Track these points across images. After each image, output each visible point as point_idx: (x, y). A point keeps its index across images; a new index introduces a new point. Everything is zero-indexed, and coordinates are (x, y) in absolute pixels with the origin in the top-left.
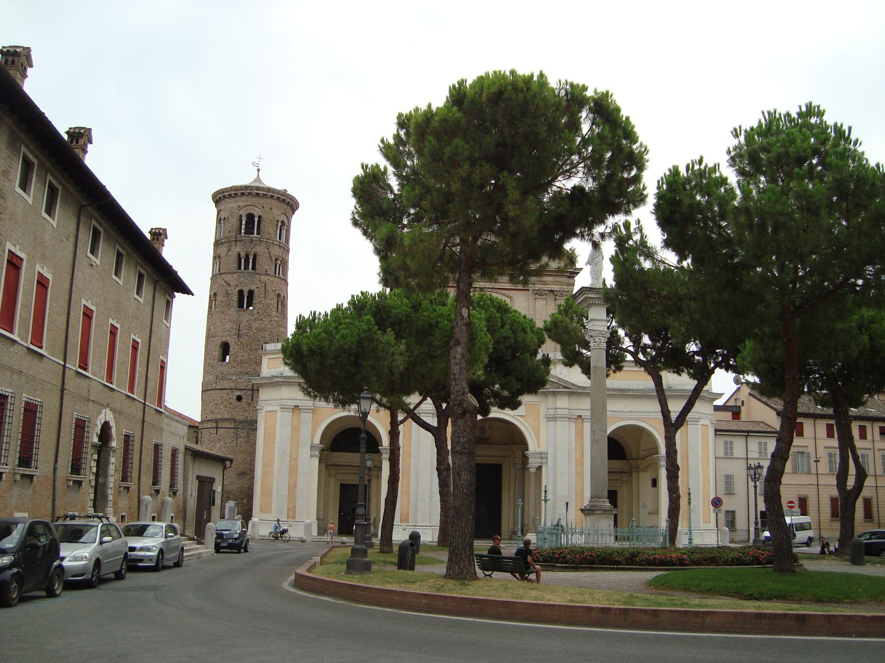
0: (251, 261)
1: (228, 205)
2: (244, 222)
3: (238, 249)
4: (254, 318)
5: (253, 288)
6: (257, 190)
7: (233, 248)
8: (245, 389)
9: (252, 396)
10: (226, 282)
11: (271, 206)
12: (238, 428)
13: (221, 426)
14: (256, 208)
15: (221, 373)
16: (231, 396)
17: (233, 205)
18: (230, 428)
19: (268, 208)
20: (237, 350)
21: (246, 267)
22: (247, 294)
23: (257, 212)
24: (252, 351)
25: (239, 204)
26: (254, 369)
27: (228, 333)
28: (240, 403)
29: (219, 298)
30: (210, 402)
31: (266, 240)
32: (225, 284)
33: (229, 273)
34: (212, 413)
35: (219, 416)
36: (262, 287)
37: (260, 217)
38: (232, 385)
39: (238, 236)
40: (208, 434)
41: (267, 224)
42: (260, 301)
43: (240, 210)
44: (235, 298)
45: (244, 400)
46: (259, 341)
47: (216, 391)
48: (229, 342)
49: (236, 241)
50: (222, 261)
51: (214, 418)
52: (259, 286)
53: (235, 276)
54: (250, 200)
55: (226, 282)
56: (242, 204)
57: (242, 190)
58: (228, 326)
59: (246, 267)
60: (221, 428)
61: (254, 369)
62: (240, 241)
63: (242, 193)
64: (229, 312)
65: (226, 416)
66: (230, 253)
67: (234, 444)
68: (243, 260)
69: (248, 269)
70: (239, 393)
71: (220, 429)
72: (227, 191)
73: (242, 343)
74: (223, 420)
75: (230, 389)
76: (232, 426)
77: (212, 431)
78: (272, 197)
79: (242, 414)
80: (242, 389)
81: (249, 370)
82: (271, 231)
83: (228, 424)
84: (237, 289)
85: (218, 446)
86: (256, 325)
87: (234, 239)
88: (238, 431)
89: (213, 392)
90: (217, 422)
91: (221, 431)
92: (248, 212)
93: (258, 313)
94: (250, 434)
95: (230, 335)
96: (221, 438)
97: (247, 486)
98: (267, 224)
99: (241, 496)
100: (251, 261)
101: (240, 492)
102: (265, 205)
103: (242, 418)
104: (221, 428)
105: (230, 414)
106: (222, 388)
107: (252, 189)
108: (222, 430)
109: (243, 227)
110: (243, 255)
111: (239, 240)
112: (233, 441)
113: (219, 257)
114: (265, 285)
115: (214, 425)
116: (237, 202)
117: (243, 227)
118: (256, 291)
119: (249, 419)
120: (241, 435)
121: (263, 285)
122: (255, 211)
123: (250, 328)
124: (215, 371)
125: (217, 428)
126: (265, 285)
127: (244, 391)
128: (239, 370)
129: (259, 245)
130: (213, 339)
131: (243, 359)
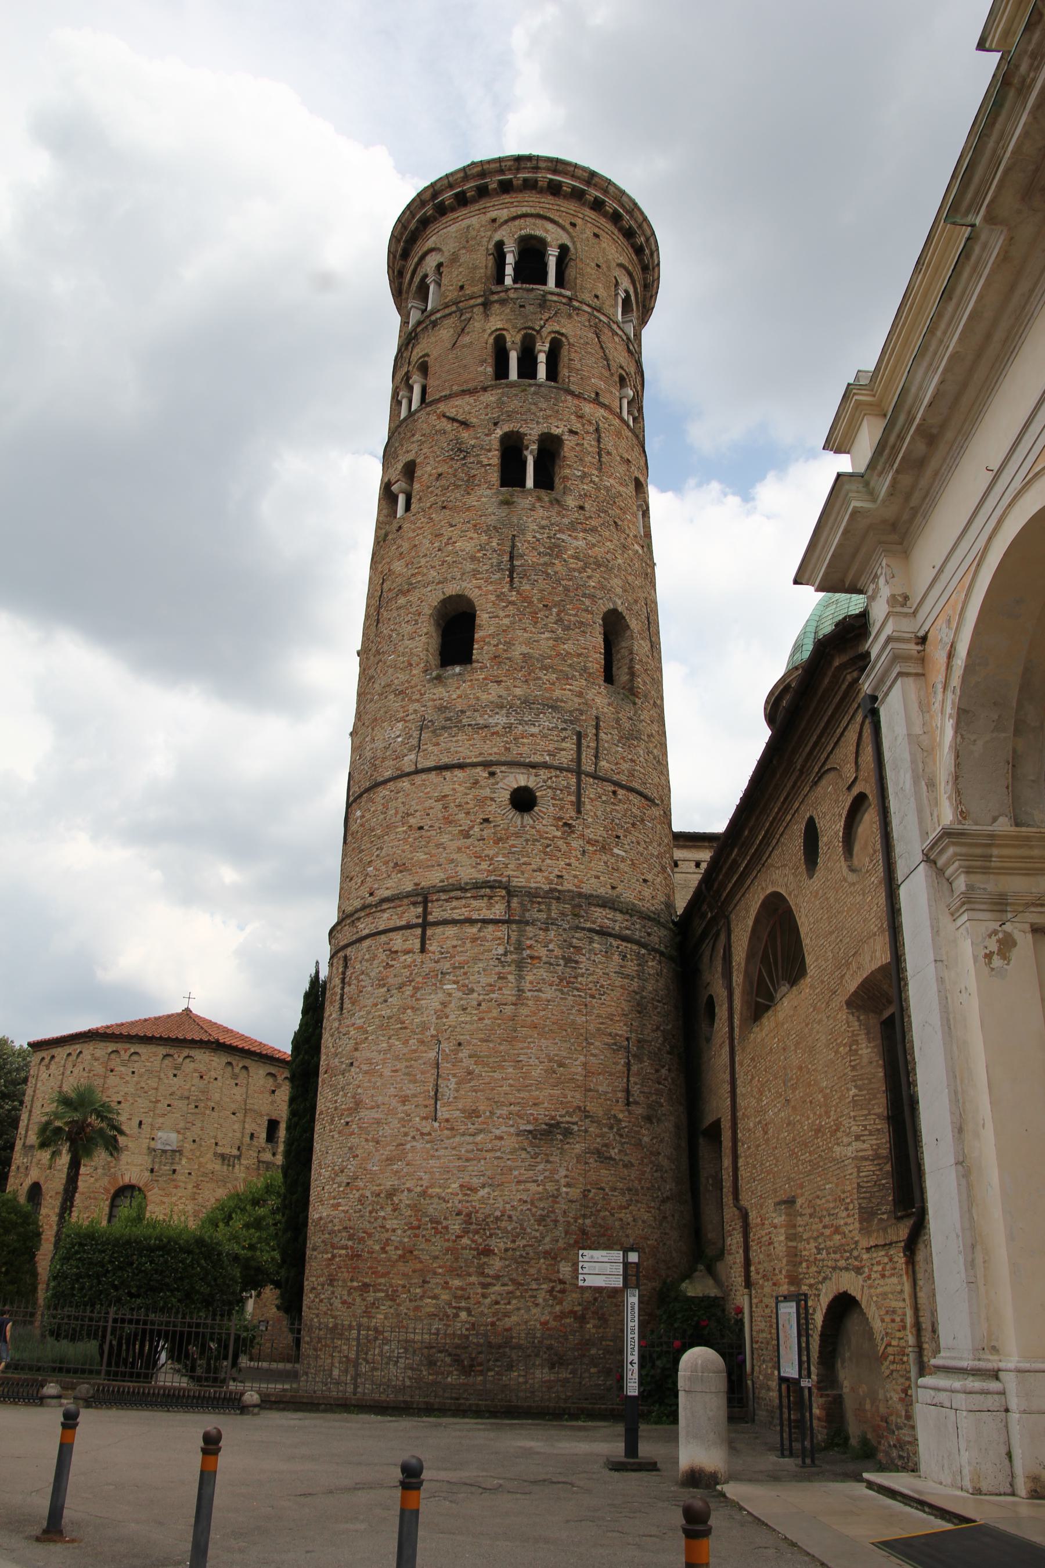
0: (542, 358)
1: (453, 228)
2: (510, 259)
3: (496, 323)
4: (566, 521)
5: (556, 431)
6: (555, 172)
7: (477, 324)
8: (545, 766)
9: (579, 796)
10: (453, 420)
11: (597, 231)
12: (523, 922)
13: (446, 915)
14: (550, 226)
15: (441, 709)
16: (487, 792)
17: (474, 221)
18: (485, 922)
19: (589, 233)
20: (506, 621)
21: (528, 369)
22: (534, 447)
23: (553, 236)
24: (567, 628)
25: (493, 214)
26: (580, 695)
27: (469, 566)
28: (527, 819)
29: (425, 472)
30: (389, 827)
31: (589, 310)
32: (448, 426)
33: (464, 392)
34: (400, 867)
35: (434, 877)
36: (587, 433)
37: (564, 249)
38: (492, 749)
39: (494, 288)
40: (382, 956)
41: (589, 270)
42: (585, 475)
43: (495, 230)
44: (494, 458)
45: (546, 807)
46: (592, 597)
47: (418, 779)
48: (474, 594)
49: (486, 305)
50: (432, 382)
51: (410, 887)
52: (577, 426)
53: (490, 397)
54: (529, 203)
55: (453, 420)
56: (504, 214)
57: (501, 171)
58: (466, 545)
59: (528, 369)
60: (445, 922)
61: (580, 695)
62: (503, 302)
63: (501, 183)
64: (472, 500)
65: (467, 873)
66: (466, 339)
67: (508, 993)
68: (513, 356)
69: (533, 375)
70: (521, 779)
71: (439, 930)
72: (451, 186)
73: (527, 599)
74: (456, 889)
75: (486, 764)
76: (498, 910)
77: (398, 941)
78: (597, 205)
79: (536, 862)
80: (533, 766)
81: (558, 693)
82: (601, 292)
83: (475, 903)
84: (499, 432)
85: (432, 1001)
86: (577, 543)
87: (480, 300)
88: (521, 933)
89: (405, 784)
90: (425, 902)
91: (443, 937)
92: (523, 232)
93: (582, 508)
94: (578, 949)
95: (475, 573)
96: (446, 966)
97: (575, 1193)
98: (589, 270)
99: (547, 1245)
100: (542, 358)
101: (541, 1220)
102: (579, 222)
103: (539, 882)
104: (445, 922)
105: (484, 866)
106: (445, 760)
107: (536, 169)
108: (451, 931)
109: (509, 270)
110: (513, 340)
111: (496, 301)
112: (501, 977)
113: (424, 368)
114: (597, 430)
115: (413, 914)
116: (484, 211)
117: (509, 270)
118: (569, 441)
119: (567, 886)
120: (542, 952)
121: (591, 429)
122: (547, 231)
123: (555, 549)
124: (416, 706)
125: (425, 925)
126: (597, 430)
127: (544, 774)
128: (518, 692)
129: (570, 316)
130: (402, 601)
131: (536, 653)
